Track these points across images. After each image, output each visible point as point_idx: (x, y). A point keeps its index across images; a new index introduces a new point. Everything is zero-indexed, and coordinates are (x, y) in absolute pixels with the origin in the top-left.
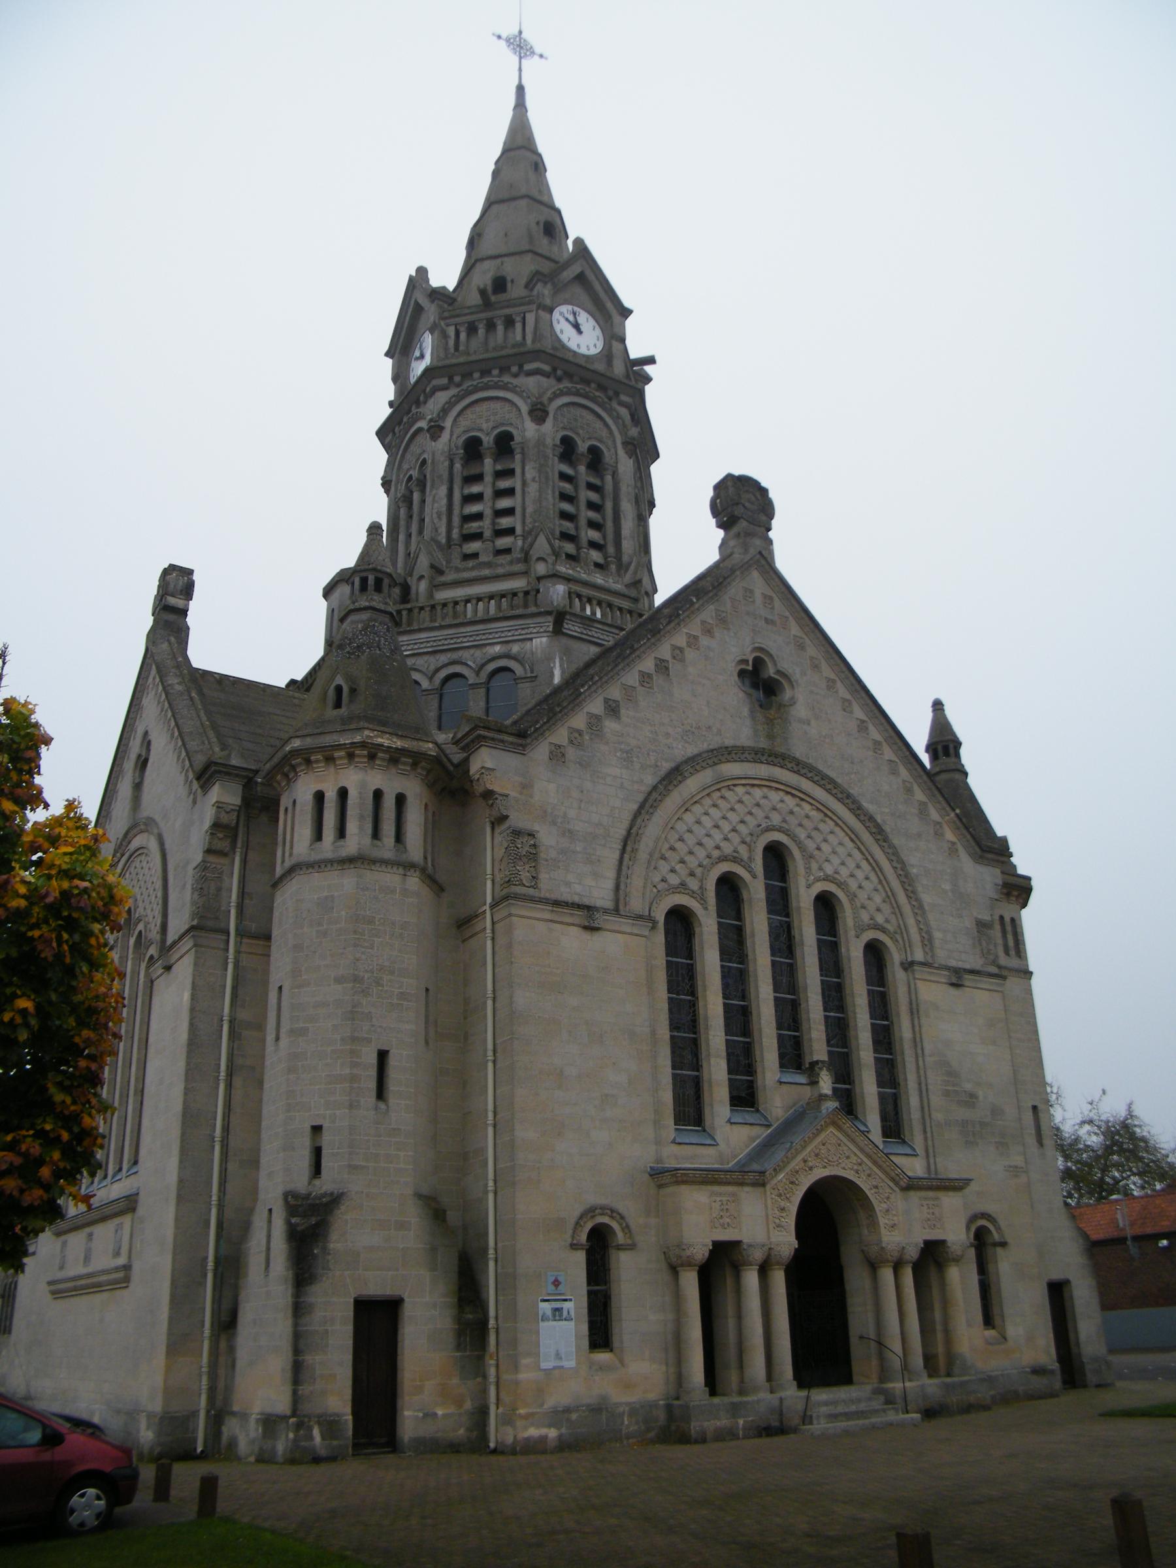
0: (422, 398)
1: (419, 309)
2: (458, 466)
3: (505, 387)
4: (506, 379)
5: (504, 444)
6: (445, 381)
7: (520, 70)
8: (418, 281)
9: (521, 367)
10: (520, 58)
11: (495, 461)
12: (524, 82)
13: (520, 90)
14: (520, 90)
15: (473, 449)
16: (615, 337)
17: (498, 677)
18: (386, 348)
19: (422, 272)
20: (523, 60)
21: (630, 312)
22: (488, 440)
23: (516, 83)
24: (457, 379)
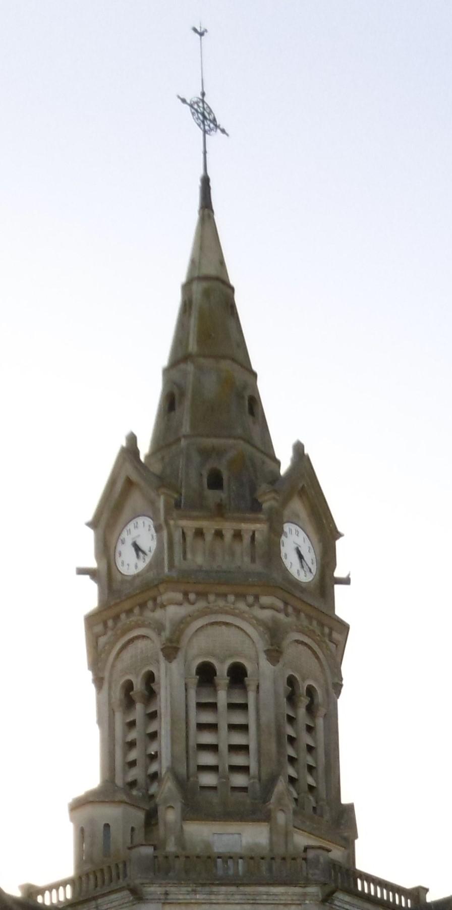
0: (150, 604)
1: (129, 483)
2: (192, 693)
3: (240, 615)
4: (242, 606)
5: (238, 675)
6: (179, 596)
7: (205, 153)
8: (130, 450)
9: (257, 598)
10: (205, 132)
11: (229, 694)
13: (206, 182)
14: (206, 182)
15: (206, 674)
16: (327, 559)
18: (90, 516)
19: (132, 439)
20: (207, 136)
22: (222, 670)
23: (201, 173)
24: (192, 597)
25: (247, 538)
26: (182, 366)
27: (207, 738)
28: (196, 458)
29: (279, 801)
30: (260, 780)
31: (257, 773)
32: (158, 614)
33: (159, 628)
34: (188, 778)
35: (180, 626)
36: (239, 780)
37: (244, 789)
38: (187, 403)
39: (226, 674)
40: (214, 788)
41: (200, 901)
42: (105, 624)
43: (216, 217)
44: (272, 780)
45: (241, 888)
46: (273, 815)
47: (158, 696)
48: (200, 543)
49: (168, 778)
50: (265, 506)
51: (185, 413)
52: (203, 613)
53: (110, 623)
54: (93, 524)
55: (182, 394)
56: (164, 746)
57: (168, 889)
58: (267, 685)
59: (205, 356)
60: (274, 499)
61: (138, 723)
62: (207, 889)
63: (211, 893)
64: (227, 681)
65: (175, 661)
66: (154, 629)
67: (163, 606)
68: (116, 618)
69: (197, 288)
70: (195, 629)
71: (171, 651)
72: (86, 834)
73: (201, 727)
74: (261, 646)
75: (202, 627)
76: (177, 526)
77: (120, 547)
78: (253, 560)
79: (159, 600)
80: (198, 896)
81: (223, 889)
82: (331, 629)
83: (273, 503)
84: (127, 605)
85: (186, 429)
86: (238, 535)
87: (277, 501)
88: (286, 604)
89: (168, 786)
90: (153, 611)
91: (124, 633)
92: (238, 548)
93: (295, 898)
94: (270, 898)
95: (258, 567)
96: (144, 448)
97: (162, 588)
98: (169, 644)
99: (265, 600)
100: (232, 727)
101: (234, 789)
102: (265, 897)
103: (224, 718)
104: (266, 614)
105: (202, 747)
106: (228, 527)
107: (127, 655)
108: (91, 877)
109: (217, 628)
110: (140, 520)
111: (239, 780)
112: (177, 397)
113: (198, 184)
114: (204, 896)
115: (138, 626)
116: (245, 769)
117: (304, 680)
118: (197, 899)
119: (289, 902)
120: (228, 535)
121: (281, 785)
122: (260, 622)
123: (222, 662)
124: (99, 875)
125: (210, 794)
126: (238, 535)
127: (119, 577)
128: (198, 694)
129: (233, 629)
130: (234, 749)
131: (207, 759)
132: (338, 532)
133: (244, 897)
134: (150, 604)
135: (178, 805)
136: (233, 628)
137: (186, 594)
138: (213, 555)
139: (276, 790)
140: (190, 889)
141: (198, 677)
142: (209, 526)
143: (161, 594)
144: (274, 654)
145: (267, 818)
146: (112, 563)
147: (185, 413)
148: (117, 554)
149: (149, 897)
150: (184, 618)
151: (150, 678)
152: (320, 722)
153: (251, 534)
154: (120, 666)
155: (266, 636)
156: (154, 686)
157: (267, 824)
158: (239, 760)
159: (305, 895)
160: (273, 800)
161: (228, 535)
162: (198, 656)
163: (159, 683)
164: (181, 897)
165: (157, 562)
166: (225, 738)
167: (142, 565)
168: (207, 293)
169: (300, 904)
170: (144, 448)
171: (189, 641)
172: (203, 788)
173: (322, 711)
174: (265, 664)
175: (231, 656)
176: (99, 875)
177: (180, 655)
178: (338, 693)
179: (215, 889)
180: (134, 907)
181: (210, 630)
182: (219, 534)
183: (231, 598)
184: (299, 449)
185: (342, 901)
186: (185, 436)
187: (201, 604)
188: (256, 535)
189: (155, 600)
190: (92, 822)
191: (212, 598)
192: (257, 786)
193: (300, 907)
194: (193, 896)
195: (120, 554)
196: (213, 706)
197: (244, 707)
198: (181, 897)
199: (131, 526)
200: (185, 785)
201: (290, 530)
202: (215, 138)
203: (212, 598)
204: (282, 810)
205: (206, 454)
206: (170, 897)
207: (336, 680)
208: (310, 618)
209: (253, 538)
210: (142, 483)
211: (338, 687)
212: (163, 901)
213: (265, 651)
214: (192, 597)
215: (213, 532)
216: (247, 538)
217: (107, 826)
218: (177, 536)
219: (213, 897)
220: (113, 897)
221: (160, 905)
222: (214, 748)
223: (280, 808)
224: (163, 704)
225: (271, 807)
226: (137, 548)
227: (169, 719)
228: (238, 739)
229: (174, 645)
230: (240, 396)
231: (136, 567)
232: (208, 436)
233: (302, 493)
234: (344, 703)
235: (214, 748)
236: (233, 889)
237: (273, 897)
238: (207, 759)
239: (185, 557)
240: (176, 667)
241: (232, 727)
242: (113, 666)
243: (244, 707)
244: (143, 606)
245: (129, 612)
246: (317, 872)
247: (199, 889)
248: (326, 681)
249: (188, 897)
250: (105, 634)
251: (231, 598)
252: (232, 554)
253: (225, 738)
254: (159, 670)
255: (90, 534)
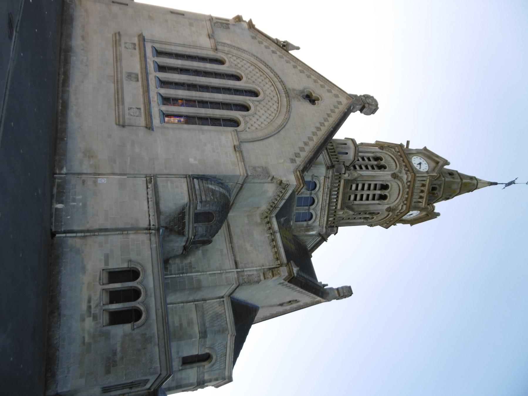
0: (407, 169)
1: (437, 163)
2: (381, 183)
5: (383, 197)
6: (409, 180)
7: (502, 184)
8: (447, 163)
9: (406, 204)
10: (506, 184)
12: (498, 185)
13: (496, 184)
14: (496, 184)
15: (385, 187)
17: (310, 217)
18: (428, 148)
21: (411, 226)
23: (498, 183)
24: (409, 184)
25: (420, 200)
26: (459, 178)
27: (366, 187)
28: (439, 183)
29: (346, 212)
30: (353, 205)
31: (354, 204)
32: (404, 172)
33: (400, 172)
34: (356, 181)
35: (401, 179)
36: (352, 197)
37: (349, 199)
38: (452, 180)
39: (385, 194)
40: (351, 189)
41: (324, 190)
42: (399, 152)
43: (488, 187)
44: (352, 210)
45: (327, 205)
46: (343, 210)
47: (379, 170)
48: (420, 185)
49: (358, 175)
50: (429, 206)
51: (448, 179)
52: (403, 187)
53: (399, 154)
54: (425, 149)
55: (453, 178)
56: (365, 173)
57: (330, 178)
58: (380, 207)
59: (461, 185)
60: (431, 209)
61: (370, 162)
62: (329, 193)
63: (327, 194)
64: (383, 194)
65: (391, 177)
66: (399, 170)
67: (406, 174)
68: (401, 156)
69: (475, 182)
70: (399, 184)
71: (395, 176)
72: (345, 145)
73: (370, 185)
74: (392, 205)
75: (399, 186)
76: (427, 178)
77: (419, 158)
78: (415, 202)
79: (408, 172)
80: (326, 189)
81: (328, 198)
82: (387, 224)
83: (430, 209)
84: (405, 160)
85: (447, 179)
86: (421, 197)
87: (430, 210)
88: (401, 213)
89: (355, 174)
90: (404, 169)
91: (396, 158)
92: (417, 197)
93: (322, 224)
94: (323, 215)
95: (413, 204)
96: (446, 167)
97: (412, 174)
98: (397, 176)
99: (405, 207)
100: (368, 196)
101: (350, 196)
102: (323, 213)
103: (371, 193)
104: (400, 207)
105: (363, 185)
106: (424, 195)
107: (390, 159)
108: (332, 147)
109: (398, 191)
110: (427, 165)
111: (352, 197)
112: (452, 176)
113: (496, 182)
114: (326, 191)
115: (400, 164)
116: (355, 199)
117: (377, 217)
118: (325, 189)
119: (321, 222)
120: (422, 194)
121: (351, 213)
122: (398, 205)
123: (389, 193)
124: (333, 150)
125: (349, 188)
126: (421, 197)
127: (411, 157)
128: (379, 184)
129: (397, 196)
130: (362, 196)
131: (360, 187)
132: (413, 225)
133: (324, 206)
134: (407, 169)
135: (349, 178)
136: (397, 196)
137: (410, 182)
138: (418, 189)
139: (350, 211)
140: (329, 186)
141: (385, 185)
142: (426, 189)
143: (410, 173)
144: (389, 210)
145: (342, 209)
146: (415, 155)
147: (448, 179)
148: (417, 157)
149: (328, 171)
150: (402, 180)
151: (384, 167)
152: (362, 220)
153: (422, 202)
154: (387, 156)
155: (395, 207)
156: (383, 169)
157: (340, 208)
158: (358, 197)
159: (323, 228)
160: (347, 210)
161: (422, 194)
162: (391, 185)
163: (384, 171)
164: (327, 183)
165: (419, 172)
166: (365, 193)
167: (415, 165)
168: (474, 185)
169: (319, 226)
170: (446, 167)
171: (396, 182)
172: (352, 186)
173: (365, 221)
174: (387, 206)
175: (390, 195)
176: (333, 150)
177: (393, 179)
178: (369, 226)
179: (328, 196)
180: (325, 165)
181: (398, 189)
182: (422, 191)
183: (406, 196)
184: (438, 214)
185: (318, 239)
186: (445, 179)
187: (406, 186)
188: (421, 204)
189: (408, 171)
190: (349, 148)
191: (407, 190)
192: (351, 204)
193: (318, 225)
194: (326, 188)
195: (417, 158)
196: (375, 189)
197: (373, 199)
198: (327, 183)
199: (425, 162)
200: (355, 179)
201: (418, 212)
202: (504, 186)
203: (407, 190)
204: (343, 213)
205: (440, 186)
206: (327, 179)
207: (373, 225)
208: (394, 218)
209: (420, 202)
210: (439, 167)
211: (371, 225)
212: (326, 176)
213: (390, 207)
214: (409, 184)
215: (424, 190)
216: (420, 200)
217: (347, 153)
218: (424, 179)
219: (325, 195)
220: (328, 157)
221: (325, 175)
222: (363, 189)
223: (344, 212)
224: (377, 172)
225: (345, 210)
226: (420, 164)
227: (375, 175)
228: (365, 197)
229: (396, 177)
230: (450, 196)
231: (415, 163)
232: (444, 186)
233: (427, 215)
234: (365, 228)
235: (363, 189)
236: (328, 202)
237: (323, 217)
238: (360, 187)
239: (418, 181)
240: (390, 177)
241: (368, 196)
242: (386, 154)
243: (373, 199)
244: (406, 166)
245: (403, 161)
246: (330, 231)
247: (329, 190)
248: (374, 222)
249: (327, 185)
250: (395, 151)
251: (406, 196)
252: (416, 196)
253: (365, 193)
254: (388, 171)
255: (421, 147)
